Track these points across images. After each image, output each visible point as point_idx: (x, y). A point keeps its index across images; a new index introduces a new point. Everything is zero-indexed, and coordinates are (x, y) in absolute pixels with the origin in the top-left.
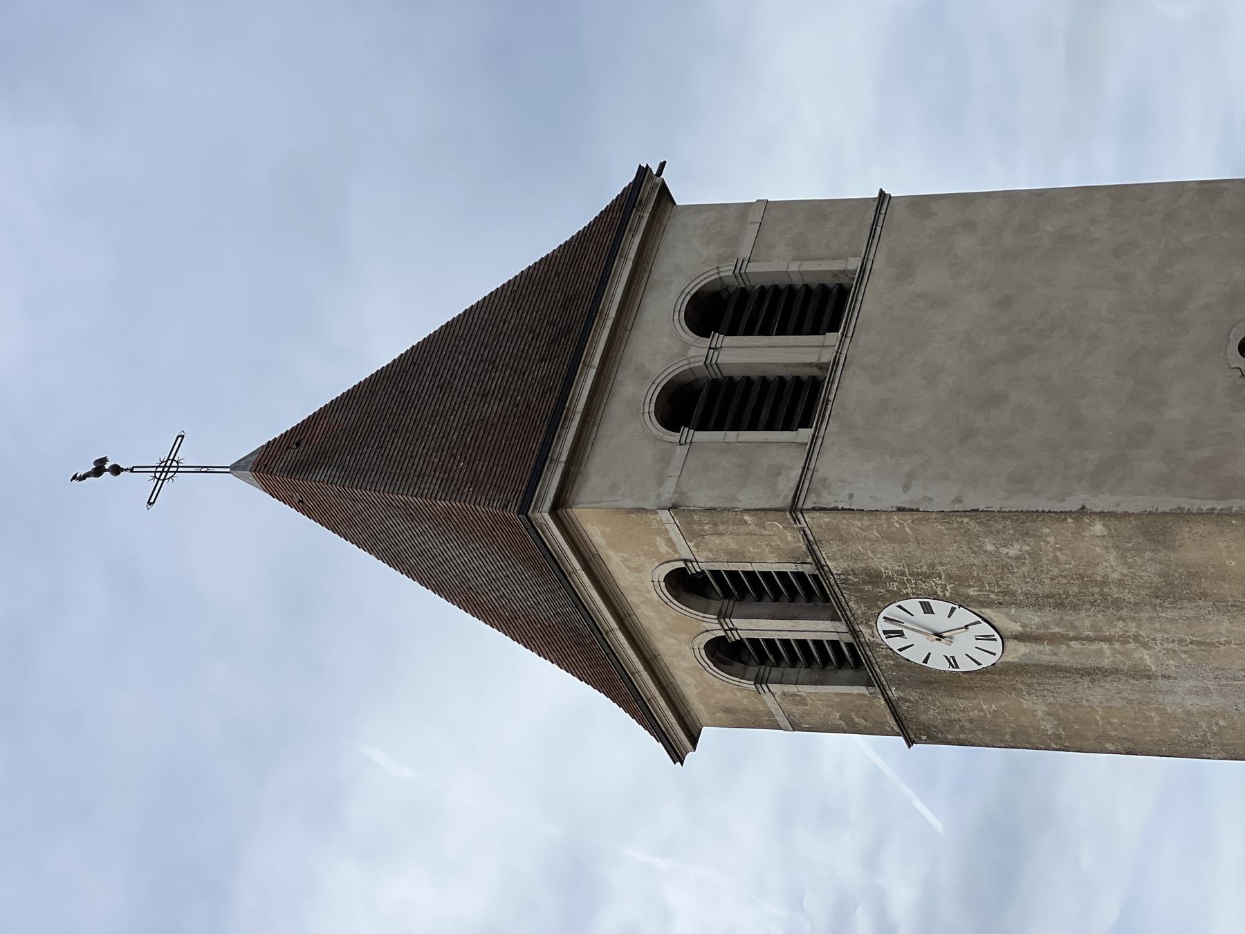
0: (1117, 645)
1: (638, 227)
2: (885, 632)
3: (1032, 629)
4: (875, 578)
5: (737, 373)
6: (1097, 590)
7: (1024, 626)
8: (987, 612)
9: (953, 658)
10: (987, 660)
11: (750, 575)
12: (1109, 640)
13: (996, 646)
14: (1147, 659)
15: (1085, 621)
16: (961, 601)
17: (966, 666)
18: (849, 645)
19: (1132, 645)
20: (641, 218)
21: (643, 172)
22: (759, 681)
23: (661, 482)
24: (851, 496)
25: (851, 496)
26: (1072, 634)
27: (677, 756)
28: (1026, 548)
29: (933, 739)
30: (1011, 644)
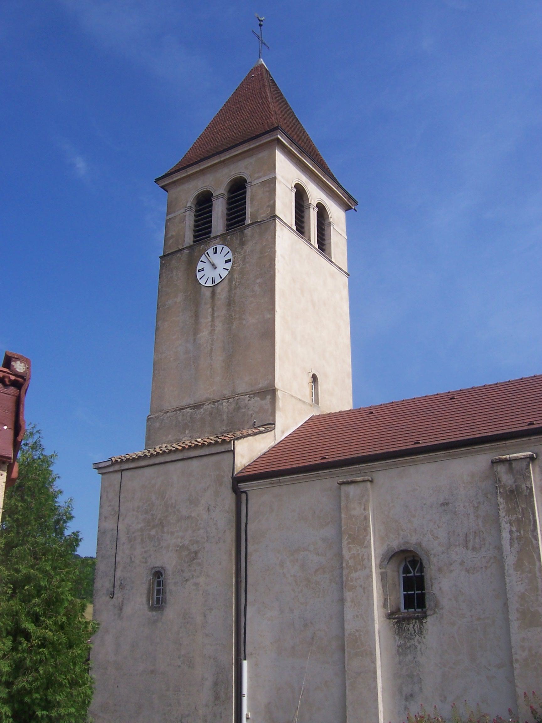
0: (210, 324)
1: (344, 196)
2: (216, 248)
3: (217, 296)
4: (242, 244)
5: (306, 215)
6: (237, 316)
7: (219, 293)
8: (226, 281)
9: (203, 270)
10: (202, 282)
11: (245, 203)
12: (213, 320)
13: (209, 284)
14: (204, 334)
15: (222, 312)
16: (232, 272)
17: (199, 275)
18: (210, 237)
19: (209, 328)
20: (346, 198)
21: (356, 203)
22: (224, 190)
23: (282, 177)
24: (279, 237)
25: (279, 237)
26: (215, 309)
27: (157, 180)
28: (258, 293)
29: (162, 265)
30: (211, 289)
